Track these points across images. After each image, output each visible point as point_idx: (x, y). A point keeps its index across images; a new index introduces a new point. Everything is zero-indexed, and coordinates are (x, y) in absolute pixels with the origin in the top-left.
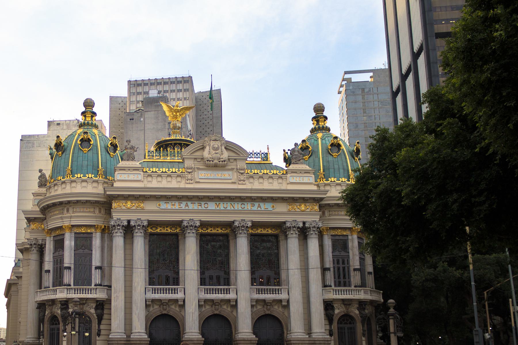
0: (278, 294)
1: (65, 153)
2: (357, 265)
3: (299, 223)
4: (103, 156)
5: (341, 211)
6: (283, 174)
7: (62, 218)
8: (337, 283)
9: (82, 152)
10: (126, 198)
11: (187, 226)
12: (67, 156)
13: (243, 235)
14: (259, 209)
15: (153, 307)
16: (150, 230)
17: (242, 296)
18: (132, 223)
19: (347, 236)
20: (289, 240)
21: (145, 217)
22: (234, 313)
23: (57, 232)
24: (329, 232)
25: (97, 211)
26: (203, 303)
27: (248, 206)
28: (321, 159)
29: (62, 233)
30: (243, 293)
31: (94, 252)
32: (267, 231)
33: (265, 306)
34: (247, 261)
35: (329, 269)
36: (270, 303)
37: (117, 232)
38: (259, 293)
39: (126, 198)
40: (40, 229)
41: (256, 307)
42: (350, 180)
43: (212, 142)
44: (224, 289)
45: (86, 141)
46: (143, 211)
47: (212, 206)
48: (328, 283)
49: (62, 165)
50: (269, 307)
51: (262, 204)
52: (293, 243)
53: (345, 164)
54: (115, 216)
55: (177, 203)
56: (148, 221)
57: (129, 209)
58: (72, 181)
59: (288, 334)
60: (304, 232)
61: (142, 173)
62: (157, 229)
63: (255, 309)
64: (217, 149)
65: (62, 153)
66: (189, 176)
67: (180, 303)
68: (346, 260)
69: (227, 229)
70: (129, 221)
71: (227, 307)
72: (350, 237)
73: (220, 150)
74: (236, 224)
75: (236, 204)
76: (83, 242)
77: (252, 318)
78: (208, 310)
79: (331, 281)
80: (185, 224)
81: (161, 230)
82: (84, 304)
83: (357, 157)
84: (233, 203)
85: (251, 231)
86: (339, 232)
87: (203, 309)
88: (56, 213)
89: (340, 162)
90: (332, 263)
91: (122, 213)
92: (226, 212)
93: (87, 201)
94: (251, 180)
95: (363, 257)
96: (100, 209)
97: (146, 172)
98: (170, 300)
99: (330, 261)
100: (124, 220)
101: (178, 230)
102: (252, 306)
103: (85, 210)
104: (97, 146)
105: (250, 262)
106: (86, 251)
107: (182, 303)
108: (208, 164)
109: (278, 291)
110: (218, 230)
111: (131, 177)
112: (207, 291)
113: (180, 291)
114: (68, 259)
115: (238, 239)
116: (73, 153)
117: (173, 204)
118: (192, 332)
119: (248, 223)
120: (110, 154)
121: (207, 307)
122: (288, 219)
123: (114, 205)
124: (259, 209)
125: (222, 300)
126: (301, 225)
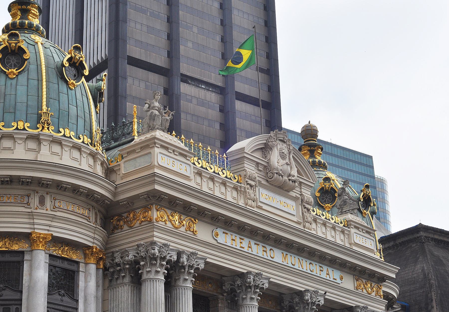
7: (31, 215)
9: (65, 86)
29: (15, 247)
37: (157, 272)
47: (278, 256)
51: (330, 270)
57: (177, 228)
84: (301, 258)
88: (5, 199)
91: (167, 234)
93: (90, 194)
94: (314, 225)
96: (96, 214)
97: (194, 164)
100: (172, 250)
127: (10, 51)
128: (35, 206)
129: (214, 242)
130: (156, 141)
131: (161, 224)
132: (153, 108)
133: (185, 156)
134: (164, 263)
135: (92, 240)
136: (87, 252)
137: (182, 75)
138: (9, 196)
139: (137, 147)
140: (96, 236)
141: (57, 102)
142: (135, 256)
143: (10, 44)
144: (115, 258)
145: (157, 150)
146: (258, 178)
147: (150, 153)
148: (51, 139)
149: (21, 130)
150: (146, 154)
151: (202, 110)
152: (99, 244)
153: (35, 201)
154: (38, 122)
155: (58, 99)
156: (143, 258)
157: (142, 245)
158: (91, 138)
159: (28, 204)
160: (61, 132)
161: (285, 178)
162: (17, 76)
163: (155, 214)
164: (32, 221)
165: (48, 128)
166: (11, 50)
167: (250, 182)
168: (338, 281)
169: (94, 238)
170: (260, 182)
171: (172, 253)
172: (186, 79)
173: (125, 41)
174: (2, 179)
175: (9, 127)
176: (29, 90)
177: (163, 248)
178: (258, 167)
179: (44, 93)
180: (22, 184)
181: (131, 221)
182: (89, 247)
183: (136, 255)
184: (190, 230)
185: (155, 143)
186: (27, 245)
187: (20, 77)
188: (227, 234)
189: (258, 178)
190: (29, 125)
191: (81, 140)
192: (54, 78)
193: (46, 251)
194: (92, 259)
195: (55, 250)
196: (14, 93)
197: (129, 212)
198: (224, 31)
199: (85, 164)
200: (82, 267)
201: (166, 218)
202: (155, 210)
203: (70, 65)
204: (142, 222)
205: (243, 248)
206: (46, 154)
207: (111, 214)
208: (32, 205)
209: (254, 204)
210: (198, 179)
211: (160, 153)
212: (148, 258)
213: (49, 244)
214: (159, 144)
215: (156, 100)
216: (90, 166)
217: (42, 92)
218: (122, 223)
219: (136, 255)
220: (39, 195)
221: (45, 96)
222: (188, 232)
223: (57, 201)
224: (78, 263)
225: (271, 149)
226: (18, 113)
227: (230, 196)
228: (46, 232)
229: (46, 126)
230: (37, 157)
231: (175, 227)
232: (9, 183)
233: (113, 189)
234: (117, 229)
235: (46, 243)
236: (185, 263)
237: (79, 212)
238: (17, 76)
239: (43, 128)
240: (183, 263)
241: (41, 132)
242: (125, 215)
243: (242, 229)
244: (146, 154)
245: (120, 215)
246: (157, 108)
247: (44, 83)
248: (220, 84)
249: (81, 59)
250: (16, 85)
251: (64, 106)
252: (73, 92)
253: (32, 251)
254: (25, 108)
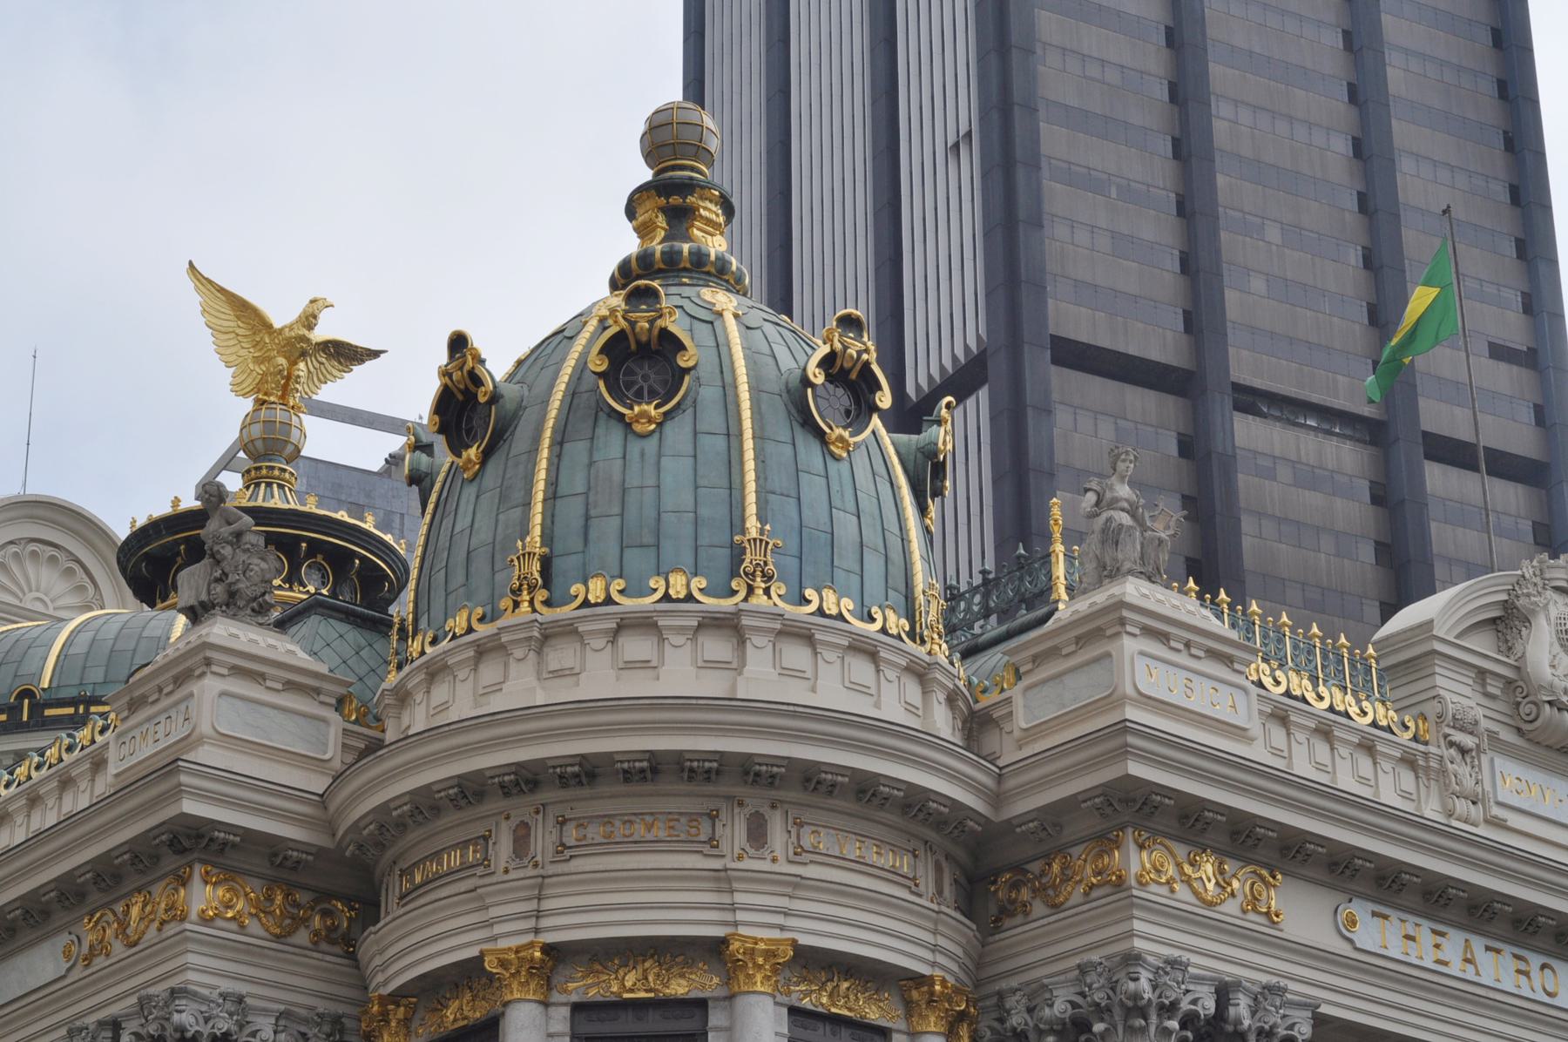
7: (723, 880)
9: (815, 447)
23: (631, 983)
29: (678, 988)
39: (1193, 825)
40: (254, 926)
45: (844, 372)
55: (1424, 931)
57: (1210, 905)
88: (639, 831)
93: (914, 803)
96: (938, 869)
97: (1260, 684)
100: (1198, 979)
127: (633, 346)
128: (737, 851)
129: (1343, 948)
130: (1125, 613)
131: (1156, 893)
132: (1113, 504)
133: (1228, 660)
134: (1174, 1024)
135: (928, 956)
136: (915, 995)
137: (1237, 388)
138: (649, 819)
139: (1064, 637)
140: (942, 941)
141: (793, 501)
142: (1074, 1005)
143: (632, 324)
144: (1008, 1012)
145: (1130, 645)
146: (1484, 724)
147: (1108, 655)
148: (779, 626)
149: (678, 600)
150: (1096, 660)
151: (1311, 502)
152: (954, 967)
153: (734, 833)
154: (734, 573)
155: (794, 494)
156: (1101, 1011)
157: (1094, 966)
158: (910, 615)
159: (712, 841)
160: (809, 602)
162: (660, 425)
163: (1134, 860)
164: (726, 899)
165: (767, 591)
166: (638, 342)
167: (1458, 737)
169: (934, 948)
170: (1492, 736)
171: (1199, 988)
172: (1250, 400)
173: (1040, 288)
174: (626, 765)
175: (641, 595)
176: (701, 472)
177: (1167, 973)
178: (1484, 685)
179: (750, 476)
180: (690, 779)
181: (1054, 887)
182: (919, 980)
183: (1079, 1000)
184: (1255, 910)
185: (1122, 622)
186: (716, 980)
187: (668, 427)
188: (1385, 917)
189: (1484, 724)
190: (704, 584)
191: (878, 625)
192: (780, 426)
193: (779, 998)
194: (932, 1019)
195: (808, 994)
196: (651, 481)
197: (1048, 858)
198: (1372, 230)
199: (894, 701)
201: (1171, 870)
202: (1132, 847)
203: (830, 378)
204: (1092, 887)
205: (1445, 964)
206: (764, 675)
207: (988, 867)
208: (725, 847)
209: (1476, 812)
210: (1278, 736)
211: (1142, 653)
212: (1117, 1011)
213: (787, 973)
214: (1134, 623)
215: (1122, 478)
216: (910, 708)
217: (742, 474)
218: (1025, 894)
219: (1079, 1000)
220: (748, 810)
221: (751, 487)
222: (1252, 916)
223: (806, 830)
225: (1526, 621)
226: (666, 545)
227: (1391, 787)
228: (776, 934)
229: (760, 583)
230: (734, 687)
231: (1203, 901)
232: (649, 775)
233: (988, 781)
234: (1012, 915)
235: (775, 971)
236: (1247, 1023)
237: (881, 862)
238: (660, 425)
239: (751, 590)
240: (1238, 1022)
241: (743, 606)
242: (1035, 867)
243: (1437, 901)
244: (1096, 660)
245: (1019, 868)
246: (1126, 505)
247: (749, 444)
248: (1367, 411)
249: (865, 356)
250: (659, 456)
251: (816, 513)
252: (845, 466)
253: (731, 997)
254: (688, 530)
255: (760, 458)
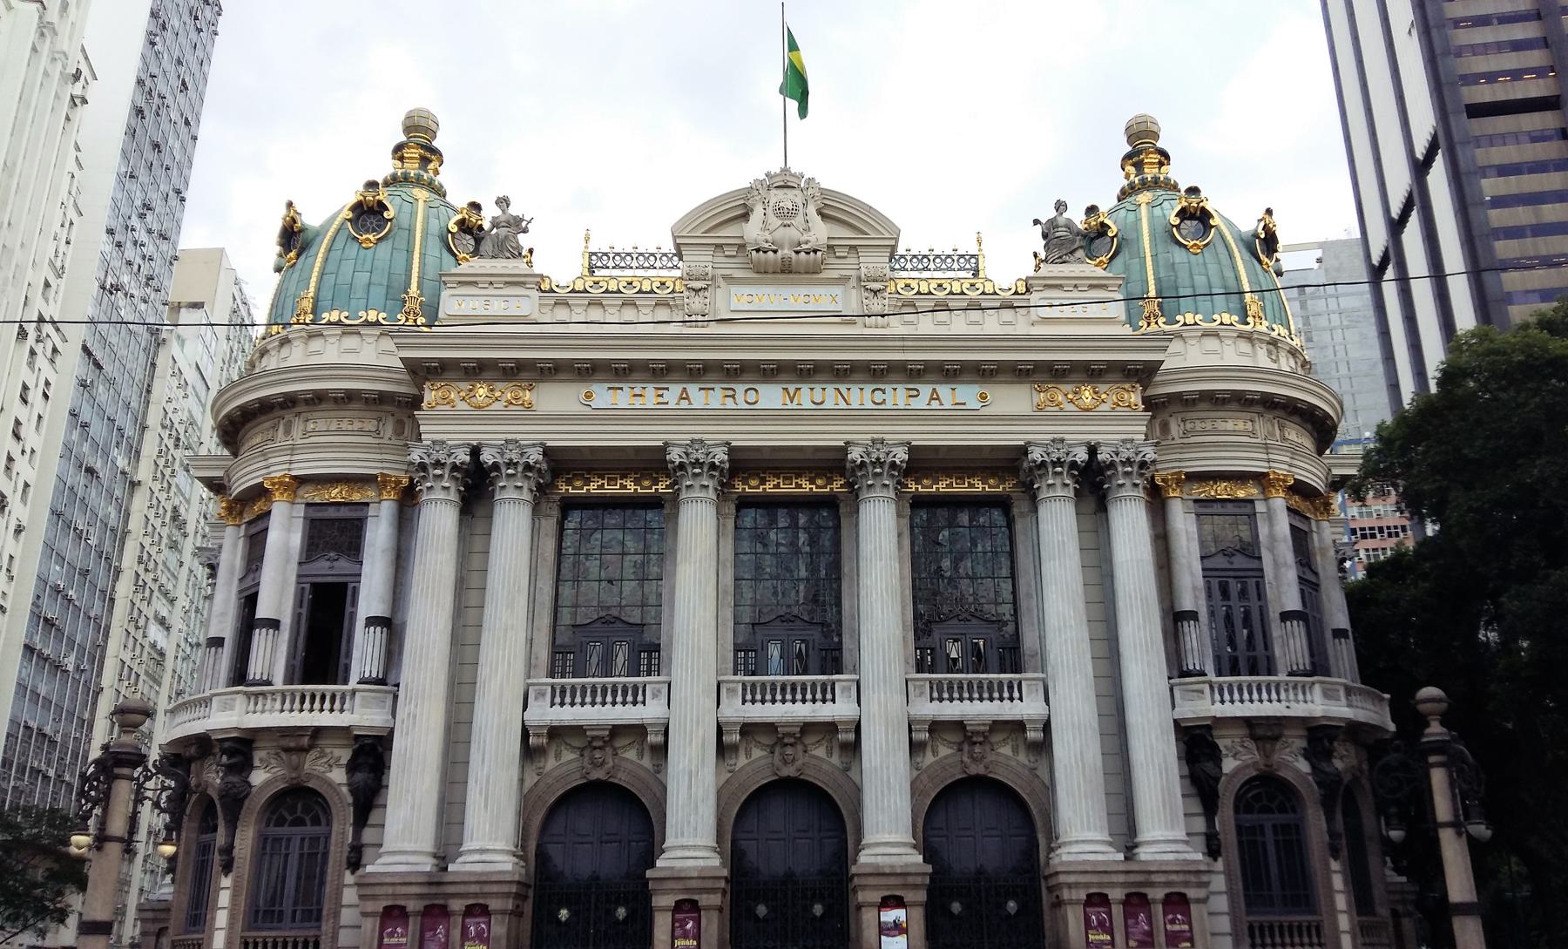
0: (1011, 699)
1: (302, 258)
2: (1293, 603)
3: (1076, 450)
4: (430, 260)
5: (1224, 420)
6: (1016, 293)
8: (1226, 665)
10: (477, 371)
11: (682, 466)
12: (310, 260)
13: (878, 492)
14: (935, 405)
15: (558, 756)
16: (563, 488)
17: (875, 708)
18: (487, 457)
19: (1252, 502)
20: (1044, 511)
21: (534, 437)
22: (853, 774)
24: (1186, 489)
25: (388, 430)
26: (736, 737)
27: (896, 396)
28: (1149, 259)
30: (882, 696)
31: (366, 568)
32: (971, 485)
33: (966, 747)
34: (895, 581)
35: (1193, 615)
36: (978, 733)
38: (941, 700)
39: (477, 371)
41: (935, 753)
42: (1250, 319)
43: (774, 191)
44: (814, 684)
46: (528, 414)
47: (771, 396)
48: (1192, 663)
49: (292, 290)
50: (977, 749)
51: (944, 390)
52: (1058, 519)
53: (1229, 274)
54: (430, 432)
55: (650, 388)
56: (548, 452)
58: (311, 336)
59: (1052, 850)
60: (1093, 482)
61: (535, 294)
62: (587, 482)
63: (929, 759)
64: (791, 213)
65: (298, 255)
66: (697, 303)
67: (651, 739)
68: (1251, 583)
69: (830, 481)
70: (475, 451)
71: (830, 753)
72: (1260, 507)
73: (800, 219)
74: (855, 454)
75: (855, 388)
76: (334, 534)
77: (915, 789)
78: (755, 763)
79: (1202, 656)
80: (675, 455)
81: (601, 487)
82: (306, 750)
83: (1269, 256)
84: (843, 388)
85: (912, 487)
86: (1221, 490)
87: (742, 761)
89: (1213, 269)
90: (1203, 595)
91: (455, 422)
92: (819, 415)
93: (350, 397)
95: (1313, 579)
97: (552, 291)
98: (617, 731)
99: (1195, 588)
100: (458, 446)
101: (661, 488)
102: (915, 747)
103: (345, 425)
104: (411, 231)
105: (908, 593)
106: (344, 565)
107: (660, 739)
108: (759, 261)
109: (1012, 692)
110: (799, 486)
111: (497, 307)
112: (753, 694)
113: (655, 696)
114: (278, 596)
115: (862, 508)
116: (329, 250)
117: (637, 391)
118: (683, 847)
119: (895, 450)
120: (454, 255)
121: (757, 753)
122: (1038, 437)
123: (430, 396)
124: (935, 405)
125: (808, 728)
126: (1082, 455)
161: (786, 252)
168: (973, 403)
170: (725, 277)
182: (376, 476)
200: (371, 511)
224: (367, 504)
255: (326, 260)
